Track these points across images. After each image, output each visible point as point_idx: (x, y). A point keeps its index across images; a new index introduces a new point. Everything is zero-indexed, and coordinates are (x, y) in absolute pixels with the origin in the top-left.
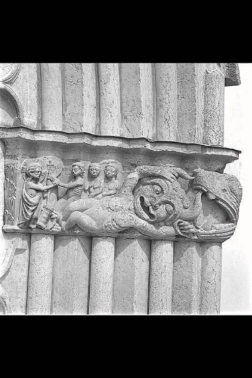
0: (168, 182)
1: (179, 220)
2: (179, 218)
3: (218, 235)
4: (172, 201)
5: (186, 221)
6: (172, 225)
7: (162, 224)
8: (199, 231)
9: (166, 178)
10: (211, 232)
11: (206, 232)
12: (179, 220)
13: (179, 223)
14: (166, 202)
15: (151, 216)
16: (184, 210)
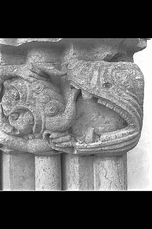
0: (26, 82)
1: (45, 132)
2: (45, 129)
3: (106, 148)
4: (29, 107)
5: (55, 132)
6: (41, 137)
7: (30, 137)
8: (77, 144)
9: (22, 78)
10: (93, 145)
11: (86, 145)
12: (45, 132)
13: (48, 135)
14: (25, 110)
15: (14, 129)
16: (48, 119)
